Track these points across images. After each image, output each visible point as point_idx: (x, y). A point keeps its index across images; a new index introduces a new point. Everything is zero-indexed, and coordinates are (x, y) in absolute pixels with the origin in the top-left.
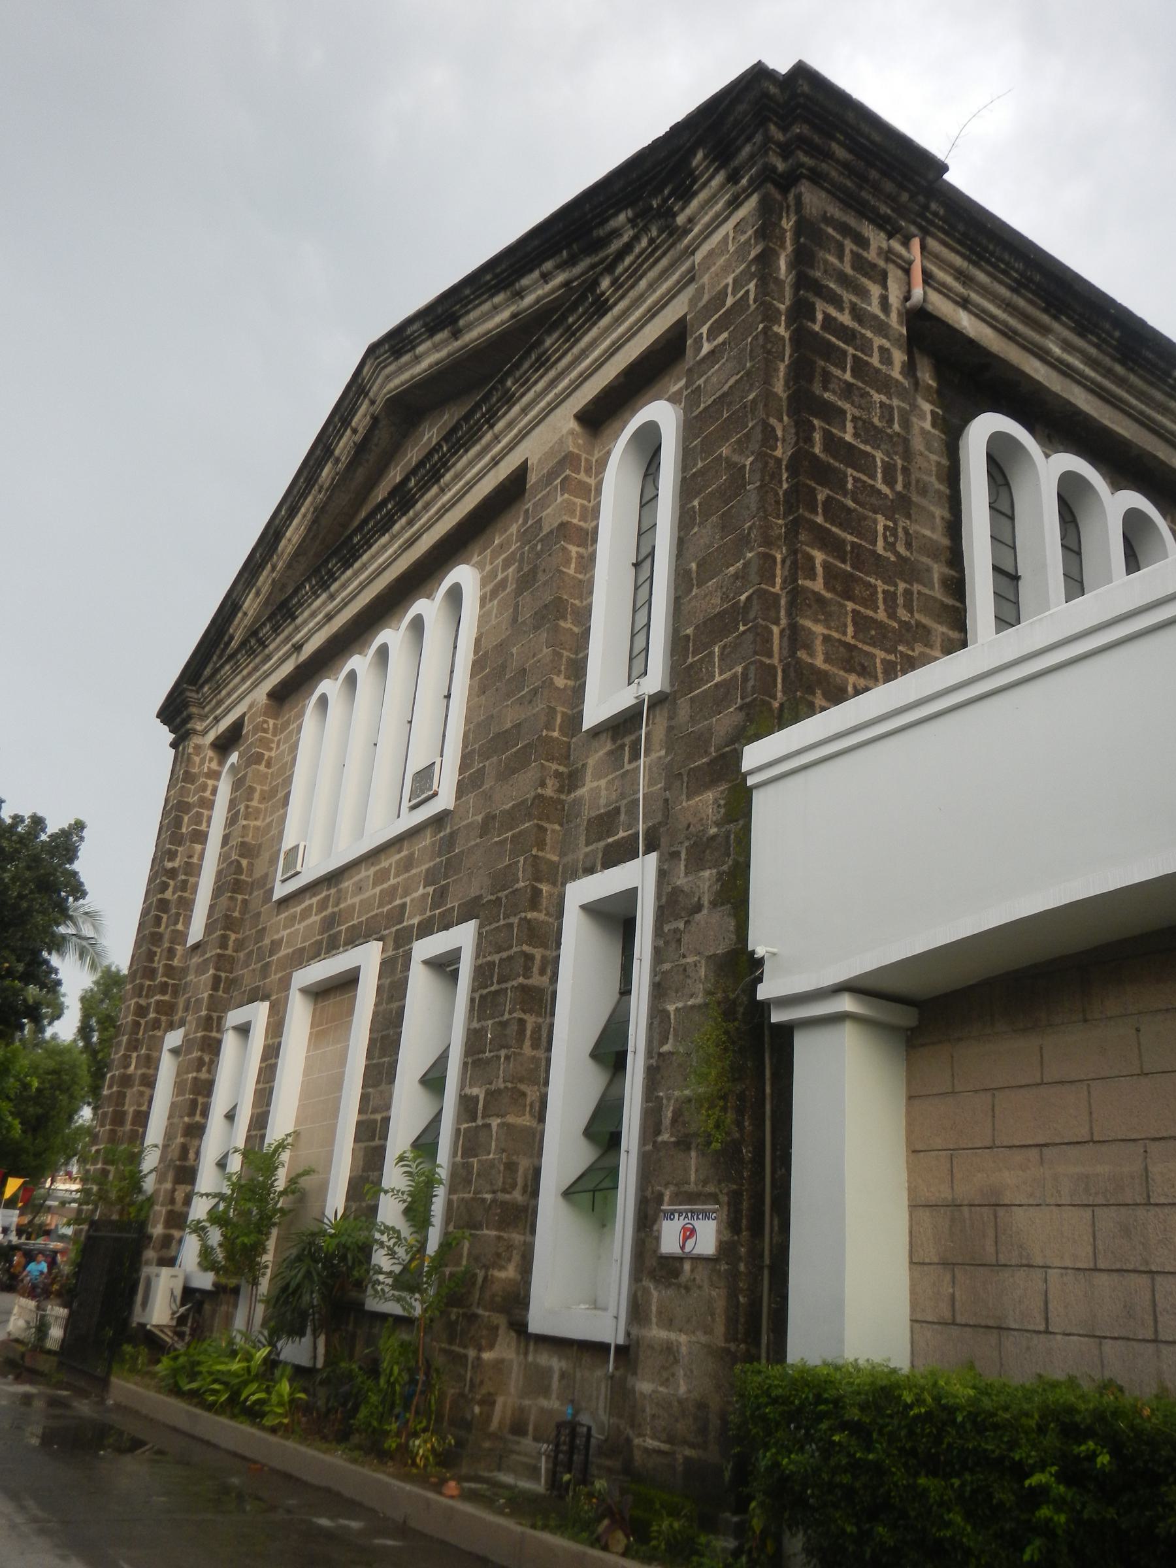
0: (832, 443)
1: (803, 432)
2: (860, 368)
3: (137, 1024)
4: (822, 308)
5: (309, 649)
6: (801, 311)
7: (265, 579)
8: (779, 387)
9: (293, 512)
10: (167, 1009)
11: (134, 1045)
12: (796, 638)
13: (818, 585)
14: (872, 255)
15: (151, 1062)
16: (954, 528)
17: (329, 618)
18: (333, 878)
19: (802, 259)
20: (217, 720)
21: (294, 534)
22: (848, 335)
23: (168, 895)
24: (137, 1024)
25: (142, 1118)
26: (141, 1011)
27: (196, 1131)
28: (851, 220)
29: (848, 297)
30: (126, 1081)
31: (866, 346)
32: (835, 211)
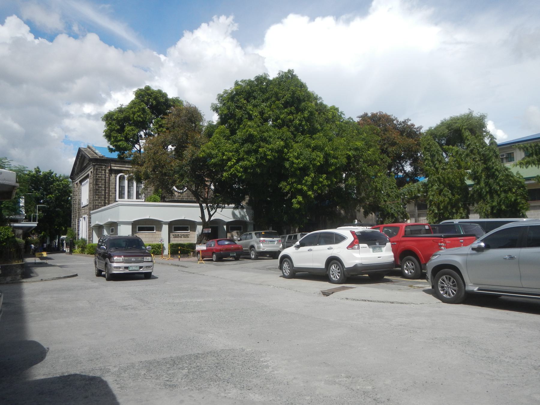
0: (98, 187)
1: (96, 187)
2: (101, 179)
3: (73, 218)
4: (97, 176)
5: (81, 178)
6: (96, 177)
7: (77, 166)
8: (95, 183)
9: (77, 160)
10: (76, 216)
11: (73, 220)
12: (96, 203)
13: (97, 198)
14: (103, 168)
15: (75, 222)
16: (116, 186)
17: (82, 176)
18: (84, 207)
19: (96, 172)
20: (76, 181)
21: (78, 163)
22: (100, 177)
23: (74, 202)
24: (73, 218)
25: (75, 228)
26: (74, 216)
27: (79, 230)
28: (101, 166)
29: (100, 174)
30: (73, 224)
31: (102, 177)
32: (99, 166)
